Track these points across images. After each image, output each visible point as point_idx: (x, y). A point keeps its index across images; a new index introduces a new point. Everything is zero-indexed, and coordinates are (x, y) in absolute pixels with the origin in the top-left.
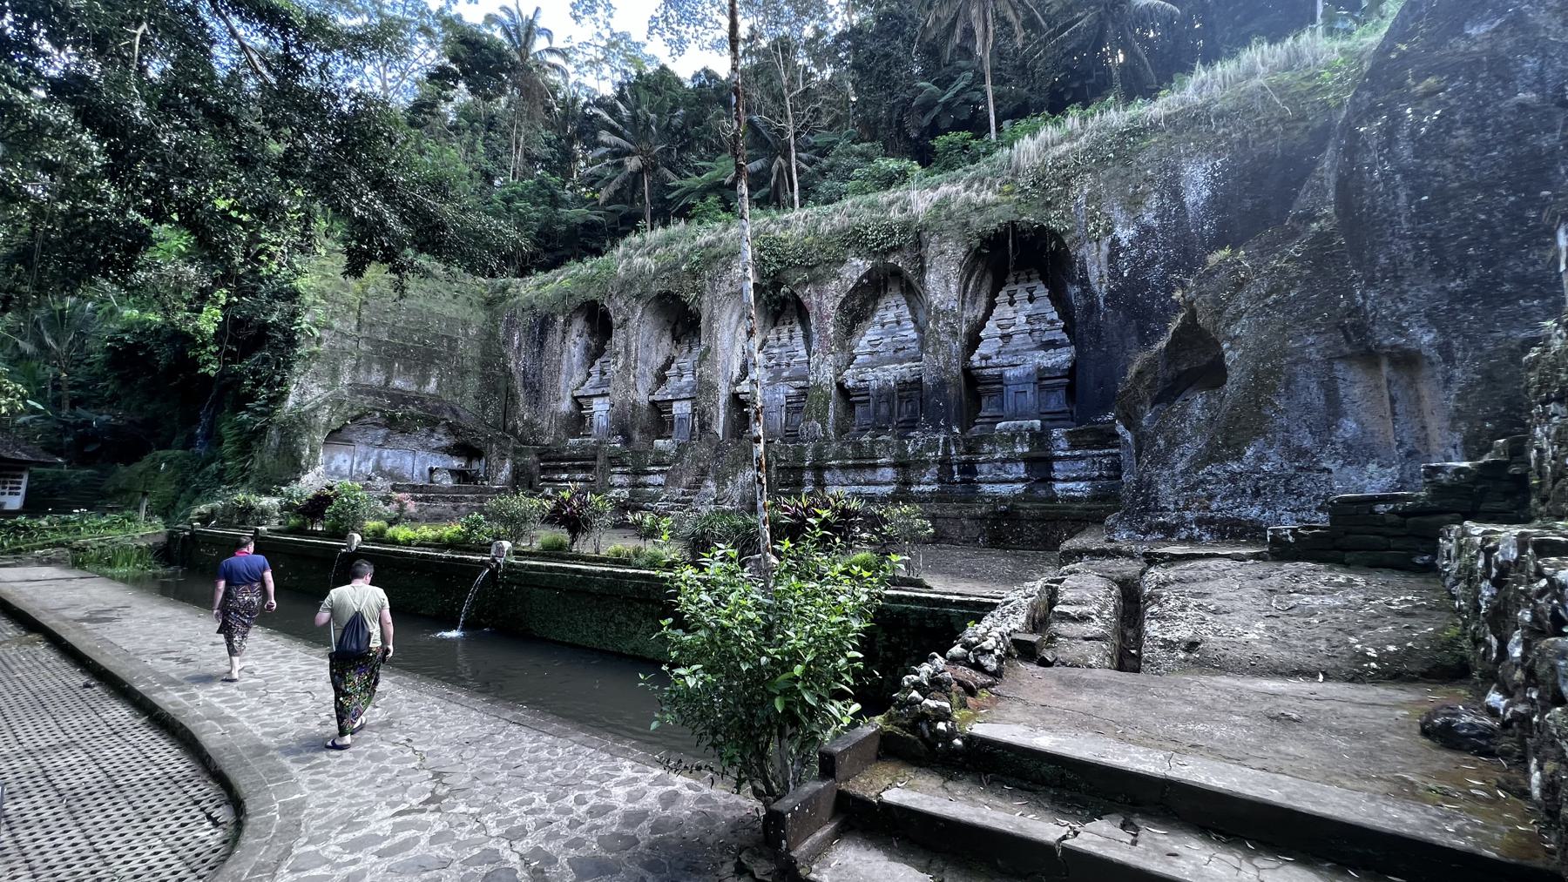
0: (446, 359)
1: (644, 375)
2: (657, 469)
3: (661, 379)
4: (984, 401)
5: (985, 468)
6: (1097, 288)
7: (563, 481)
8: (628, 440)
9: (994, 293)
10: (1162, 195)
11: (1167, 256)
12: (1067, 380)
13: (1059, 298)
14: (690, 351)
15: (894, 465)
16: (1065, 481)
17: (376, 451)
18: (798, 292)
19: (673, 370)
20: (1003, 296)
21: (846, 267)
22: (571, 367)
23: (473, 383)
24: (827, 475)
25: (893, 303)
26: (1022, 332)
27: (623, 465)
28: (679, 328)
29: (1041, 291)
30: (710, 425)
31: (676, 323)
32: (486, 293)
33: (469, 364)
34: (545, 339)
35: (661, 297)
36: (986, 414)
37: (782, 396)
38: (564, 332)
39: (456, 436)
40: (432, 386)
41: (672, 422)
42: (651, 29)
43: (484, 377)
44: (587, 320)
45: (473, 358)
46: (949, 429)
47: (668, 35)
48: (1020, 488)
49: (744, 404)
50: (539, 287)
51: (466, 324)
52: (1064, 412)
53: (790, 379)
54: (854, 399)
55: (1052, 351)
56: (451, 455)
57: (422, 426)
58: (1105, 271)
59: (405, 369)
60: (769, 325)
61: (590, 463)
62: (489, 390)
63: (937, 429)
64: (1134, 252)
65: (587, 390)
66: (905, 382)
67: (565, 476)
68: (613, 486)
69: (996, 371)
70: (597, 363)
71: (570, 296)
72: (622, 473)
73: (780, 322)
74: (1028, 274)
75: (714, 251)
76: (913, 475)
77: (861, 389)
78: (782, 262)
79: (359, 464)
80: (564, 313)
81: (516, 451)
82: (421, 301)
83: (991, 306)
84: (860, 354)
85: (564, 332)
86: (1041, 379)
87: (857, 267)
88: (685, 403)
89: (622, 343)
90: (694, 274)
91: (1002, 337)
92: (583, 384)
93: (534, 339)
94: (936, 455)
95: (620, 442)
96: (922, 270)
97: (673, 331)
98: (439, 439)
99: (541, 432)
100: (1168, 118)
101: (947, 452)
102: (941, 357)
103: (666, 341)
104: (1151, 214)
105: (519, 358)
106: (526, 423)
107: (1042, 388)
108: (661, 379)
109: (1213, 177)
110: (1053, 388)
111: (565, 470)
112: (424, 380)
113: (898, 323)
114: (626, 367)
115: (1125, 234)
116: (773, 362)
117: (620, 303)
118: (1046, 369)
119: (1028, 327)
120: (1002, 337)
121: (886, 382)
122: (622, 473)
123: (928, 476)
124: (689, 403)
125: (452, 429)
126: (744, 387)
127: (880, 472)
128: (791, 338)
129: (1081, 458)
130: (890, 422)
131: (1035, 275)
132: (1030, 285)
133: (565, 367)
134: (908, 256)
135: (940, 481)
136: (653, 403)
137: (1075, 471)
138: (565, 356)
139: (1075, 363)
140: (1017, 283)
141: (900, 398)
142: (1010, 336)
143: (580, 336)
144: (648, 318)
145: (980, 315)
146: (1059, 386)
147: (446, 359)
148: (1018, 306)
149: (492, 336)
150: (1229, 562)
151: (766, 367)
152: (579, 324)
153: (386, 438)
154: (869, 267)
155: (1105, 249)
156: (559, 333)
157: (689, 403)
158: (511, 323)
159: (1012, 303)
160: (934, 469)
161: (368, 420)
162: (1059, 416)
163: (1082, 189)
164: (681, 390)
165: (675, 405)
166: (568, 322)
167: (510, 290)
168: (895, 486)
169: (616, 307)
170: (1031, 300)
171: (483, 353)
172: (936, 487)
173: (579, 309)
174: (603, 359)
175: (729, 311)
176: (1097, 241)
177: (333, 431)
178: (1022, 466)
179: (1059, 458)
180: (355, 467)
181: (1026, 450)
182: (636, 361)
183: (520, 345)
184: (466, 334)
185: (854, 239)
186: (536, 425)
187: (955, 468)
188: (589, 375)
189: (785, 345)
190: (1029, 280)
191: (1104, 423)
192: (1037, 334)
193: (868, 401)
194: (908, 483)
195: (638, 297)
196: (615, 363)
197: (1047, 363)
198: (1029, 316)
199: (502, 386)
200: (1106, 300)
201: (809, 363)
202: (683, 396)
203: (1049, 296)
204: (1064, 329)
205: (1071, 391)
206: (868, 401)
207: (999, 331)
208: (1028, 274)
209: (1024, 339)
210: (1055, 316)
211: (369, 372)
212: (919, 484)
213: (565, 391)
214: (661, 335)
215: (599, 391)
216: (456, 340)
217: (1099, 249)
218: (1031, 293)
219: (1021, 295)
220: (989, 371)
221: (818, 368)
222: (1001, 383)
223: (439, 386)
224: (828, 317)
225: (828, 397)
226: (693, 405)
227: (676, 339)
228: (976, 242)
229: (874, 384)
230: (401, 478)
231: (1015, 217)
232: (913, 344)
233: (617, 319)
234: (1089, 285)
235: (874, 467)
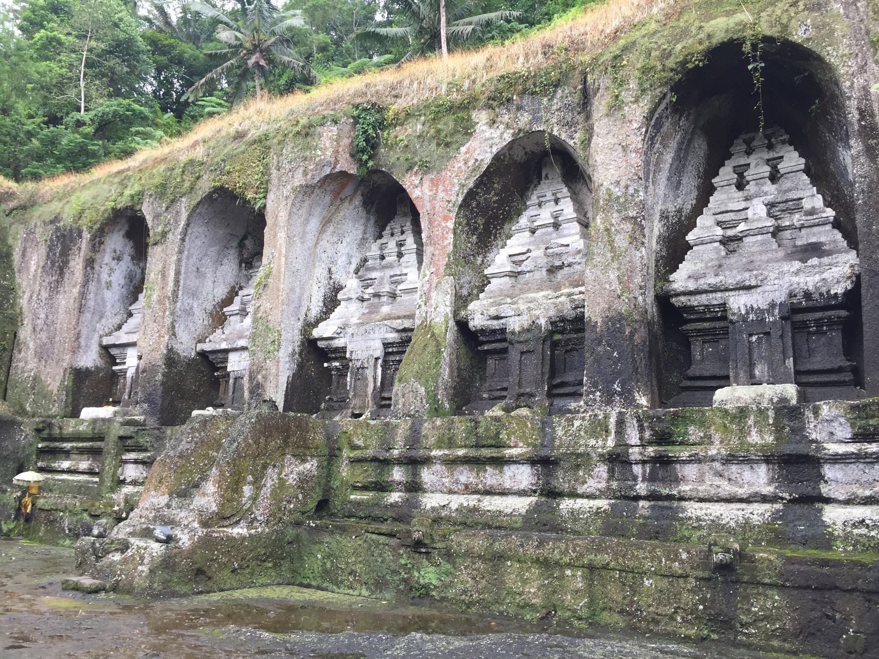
1: (189, 312)
3: (219, 319)
5: (690, 471)
7: (63, 472)
12: (843, 313)
15: (532, 462)
19: (235, 307)
20: (726, 174)
24: (427, 475)
25: (549, 196)
26: (761, 231)
31: (245, 238)
46: (629, 401)
48: (759, 513)
52: (840, 370)
53: (389, 317)
55: (814, 261)
60: (370, 236)
63: (608, 400)
65: (122, 337)
66: (563, 319)
68: (122, 482)
69: (716, 299)
76: (561, 481)
77: (494, 332)
83: (706, 191)
84: (495, 275)
91: (725, 241)
92: (119, 327)
101: (622, 444)
111: (67, 454)
116: (370, 290)
119: (770, 223)
120: (725, 241)
122: (136, 462)
126: (323, 330)
127: (509, 471)
128: (400, 255)
132: (772, 155)
133: (91, 303)
139: (857, 280)
140: (748, 153)
142: (738, 239)
143: (119, 259)
145: (688, 208)
146: (831, 323)
148: (751, 188)
151: (362, 300)
159: (740, 186)
162: (833, 378)
165: (232, 357)
168: (533, 499)
170: (774, 177)
172: (603, 504)
179: (838, 459)
181: (770, 439)
187: (637, 469)
192: (787, 234)
194: (553, 494)
198: (770, 205)
203: (807, 171)
204: (836, 224)
209: (763, 243)
210: (818, 201)
212: (574, 495)
213: (88, 339)
220: (703, 299)
235: (500, 462)
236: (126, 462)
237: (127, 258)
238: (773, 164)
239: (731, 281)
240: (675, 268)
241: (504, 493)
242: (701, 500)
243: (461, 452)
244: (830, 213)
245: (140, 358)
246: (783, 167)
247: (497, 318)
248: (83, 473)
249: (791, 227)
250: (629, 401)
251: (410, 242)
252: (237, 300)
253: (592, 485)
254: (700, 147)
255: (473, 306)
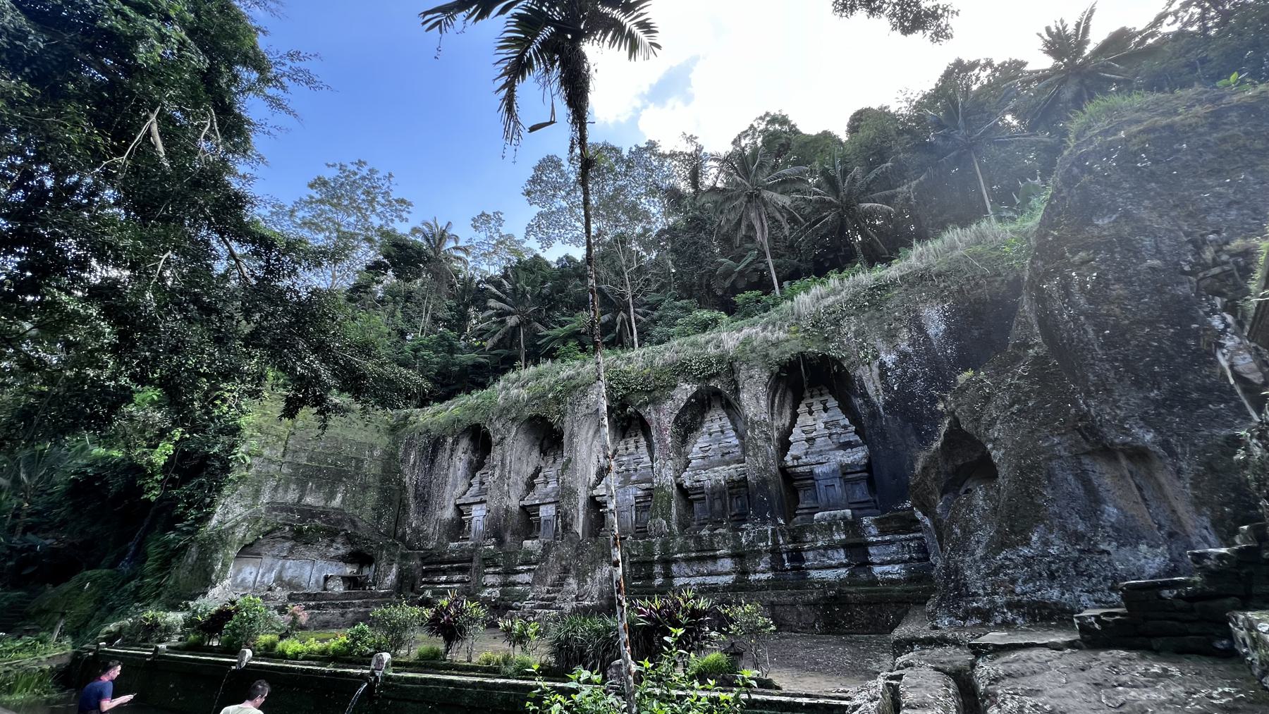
0: (352, 477)
1: (516, 484)
2: (525, 568)
3: (530, 486)
4: (801, 495)
5: (810, 555)
6: (876, 400)
7: (441, 583)
8: (500, 542)
9: (795, 406)
10: (910, 330)
11: (925, 373)
12: (866, 474)
13: (847, 408)
14: (554, 462)
15: (731, 556)
16: (882, 564)
17: (280, 562)
18: (641, 411)
19: (541, 478)
20: (802, 408)
21: (677, 390)
22: (455, 480)
23: (372, 497)
24: (674, 568)
26: (823, 436)
27: (496, 566)
28: (546, 442)
29: (832, 403)
30: (571, 525)
32: (391, 421)
33: (371, 480)
34: (436, 456)
35: (531, 419)
36: (804, 506)
37: (632, 497)
38: (452, 450)
39: (352, 545)
40: (337, 502)
41: (539, 524)
42: (528, 232)
43: (382, 491)
44: (471, 439)
45: (374, 475)
46: (775, 522)
47: (540, 235)
48: (843, 572)
49: (602, 505)
50: (434, 415)
51: (372, 447)
53: (637, 482)
54: (692, 497)
55: (849, 450)
56: (346, 562)
57: (324, 537)
58: (879, 386)
59: (316, 487)
60: (618, 438)
61: (466, 564)
62: (385, 502)
63: (764, 521)
64: (899, 371)
66: (733, 481)
67: (444, 578)
68: (485, 586)
69: (807, 469)
70: (478, 474)
71: (459, 421)
72: (494, 573)
73: (627, 435)
74: (820, 390)
75: (574, 383)
77: (697, 488)
78: (627, 389)
79: (263, 576)
80: (452, 435)
81: (404, 557)
82: (338, 431)
83: (795, 416)
85: (452, 450)
86: (845, 474)
87: (685, 390)
88: (550, 506)
89: (499, 458)
90: (557, 400)
91: (808, 440)
92: (465, 493)
93: (427, 457)
94: (767, 545)
95: (493, 544)
96: (737, 391)
97: (541, 446)
98: (337, 549)
99: (426, 538)
100: (902, 278)
101: (776, 542)
102: (760, 459)
103: (535, 453)
104: (906, 343)
105: (412, 473)
106: (414, 530)
107: (847, 481)
108: (530, 486)
109: (945, 316)
110: (855, 482)
111: (444, 572)
112: (332, 496)
113: (722, 432)
114: (501, 477)
115: (889, 359)
116: (623, 468)
117: (499, 425)
118: (847, 465)
120: (808, 440)
121: (718, 481)
122: (494, 573)
123: (762, 565)
124: (553, 507)
125: (349, 539)
126: (600, 490)
127: (720, 562)
128: (637, 447)
129: (891, 543)
130: (724, 516)
131: (825, 391)
132: (822, 399)
133: (451, 480)
134: (725, 380)
135: (773, 569)
136: (523, 508)
137: (888, 555)
138: (451, 470)
139: (870, 459)
140: (812, 397)
141: (731, 495)
143: (465, 453)
144: (521, 436)
145: (787, 424)
146: (861, 479)
147: (352, 477)
149: (392, 456)
150: (1048, 652)
151: (618, 473)
152: (464, 443)
153: (291, 551)
154: (695, 389)
155: (876, 371)
156: (448, 451)
157: (553, 507)
158: (409, 445)
159: (811, 413)
160: (767, 558)
161: (278, 534)
163: (850, 327)
164: (547, 495)
165: (542, 508)
166: (456, 442)
167: (411, 418)
168: (734, 576)
169: (495, 428)
170: (826, 410)
171: (384, 471)
172: (770, 575)
173: (465, 432)
174: (482, 472)
175: (586, 428)
176: (869, 364)
177: (246, 546)
178: (842, 551)
179: (873, 544)
180: (258, 579)
181: (843, 537)
182: (510, 472)
183: (415, 462)
184: (372, 456)
185: (681, 370)
186: (422, 532)
187: (785, 556)
188: (470, 485)
189: (632, 454)
190: (821, 395)
191: (904, 510)
192: (835, 436)
193: (704, 499)
194: (745, 572)
195: (514, 420)
196: (493, 475)
197: (848, 460)
198: (826, 423)
199: (397, 497)
200: (884, 409)
201: (652, 468)
202: (548, 500)
204: (856, 432)
205: (871, 482)
206: (704, 499)
207: (804, 436)
208: (820, 390)
210: (847, 422)
211: (286, 491)
212: (755, 572)
213: (449, 500)
214: (531, 449)
215: (478, 499)
216: (362, 461)
217: (871, 370)
218: (824, 405)
219: (817, 406)
221: (660, 472)
222: (812, 479)
223: (343, 501)
224: (666, 429)
225: (670, 497)
226: (557, 508)
227: (544, 452)
228: (776, 369)
229: (708, 484)
230: (298, 587)
231: (803, 349)
232: (737, 449)
233: (495, 439)
234: (869, 397)
235: (715, 558)
236: (487, 573)
237: (469, 452)
238: (824, 403)
239: (813, 461)
240: (786, 454)
241: (719, 574)
242: (816, 569)
243: (693, 554)
244: (853, 428)
245: (489, 511)
246: (828, 405)
247: (699, 481)
248: (456, 582)
249: (836, 433)
250: (775, 522)
251: (642, 441)
252: (541, 475)
253: (762, 566)
254: (789, 396)
255: (685, 475)
